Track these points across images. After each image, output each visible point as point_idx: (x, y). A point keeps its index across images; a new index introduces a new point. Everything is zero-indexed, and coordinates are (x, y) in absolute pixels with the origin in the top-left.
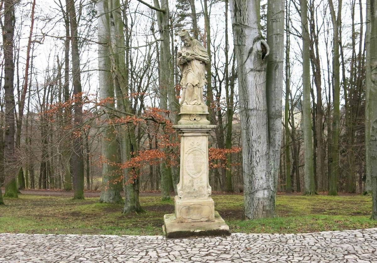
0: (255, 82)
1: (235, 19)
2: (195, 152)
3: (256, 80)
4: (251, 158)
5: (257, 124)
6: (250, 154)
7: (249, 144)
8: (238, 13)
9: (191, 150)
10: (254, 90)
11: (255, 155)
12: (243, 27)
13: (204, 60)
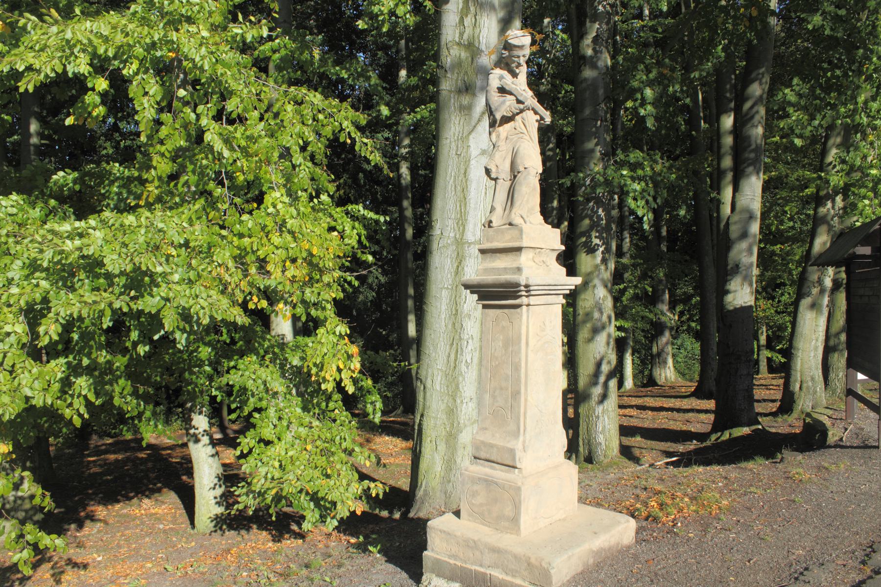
1: (457, 32)
4: (456, 356)
6: (455, 346)
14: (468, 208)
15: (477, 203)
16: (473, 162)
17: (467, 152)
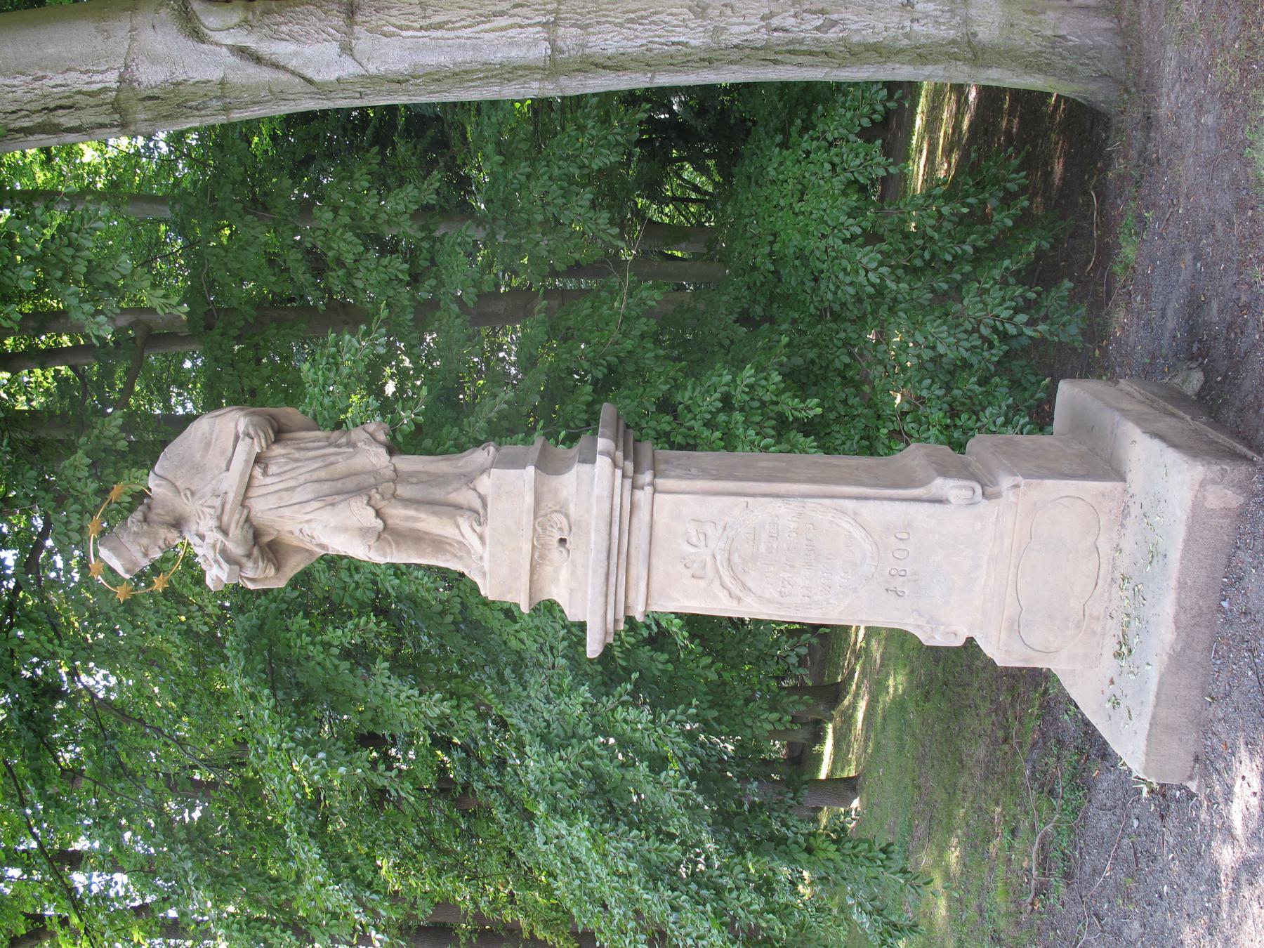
0: (410, 33)
2: (736, 558)
3: (401, 28)
4: (803, 53)
5: (631, 21)
6: (779, 57)
7: (731, 62)
8: (62, 120)
9: (728, 581)
10: (451, 34)
11: (791, 36)
12: (131, 94)
13: (247, 461)
14: (475, 66)
15: (463, 46)
16: (372, 69)
17: (352, 83)
